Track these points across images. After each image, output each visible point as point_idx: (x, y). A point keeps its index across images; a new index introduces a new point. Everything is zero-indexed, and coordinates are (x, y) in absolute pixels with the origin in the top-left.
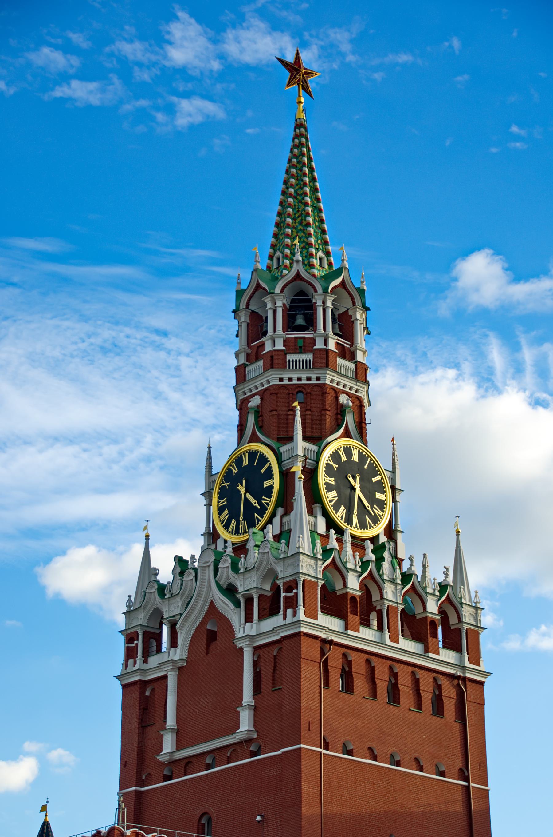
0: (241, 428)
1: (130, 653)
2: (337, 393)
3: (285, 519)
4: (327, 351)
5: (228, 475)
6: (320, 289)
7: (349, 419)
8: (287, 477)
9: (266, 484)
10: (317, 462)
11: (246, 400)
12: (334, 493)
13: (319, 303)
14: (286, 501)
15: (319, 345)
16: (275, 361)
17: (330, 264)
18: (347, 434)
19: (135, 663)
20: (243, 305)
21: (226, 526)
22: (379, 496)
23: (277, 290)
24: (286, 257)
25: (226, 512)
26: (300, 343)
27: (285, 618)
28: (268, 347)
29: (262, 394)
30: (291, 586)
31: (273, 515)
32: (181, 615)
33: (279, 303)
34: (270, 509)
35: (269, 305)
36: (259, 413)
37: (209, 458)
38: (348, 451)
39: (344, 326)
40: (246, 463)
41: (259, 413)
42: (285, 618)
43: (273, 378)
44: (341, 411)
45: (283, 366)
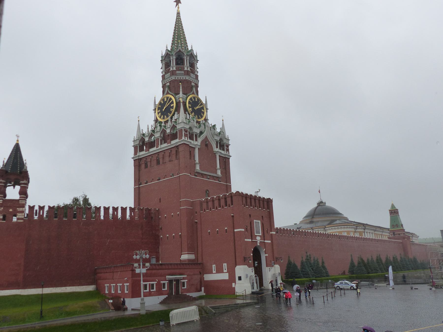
0: (163, 92)
2: (191, 82)
4: (188, 71)
5: (160, 103)
6: (185, 54)
7: (194, 89)
8: (178, 104)
9: (172, 105)
10: (186, 99)
11: (165, 84)
12: (191, 109)
13: (185, 58)
14: (177, 109)
15: (186, 69)
16: (173, 73)
17: (188, 49)
18: (193, 93)
20: (163, 59)
21: (160, 117)
22: (202, 110)
23: (174, 54)
26: (180, 68)
29: (170, 82)
30: (181, 131)
31: (174, 114)
33: (174, 58)
34: (172, 113)
35: (171, 58)
36: (169, 87)
37: (155, 100)
38: (194, 98)
39: (193, 65)
40: (166, 100)
41: (169, 87)
43: (173, 78)
44: (192, 87)
45: (176, 75)
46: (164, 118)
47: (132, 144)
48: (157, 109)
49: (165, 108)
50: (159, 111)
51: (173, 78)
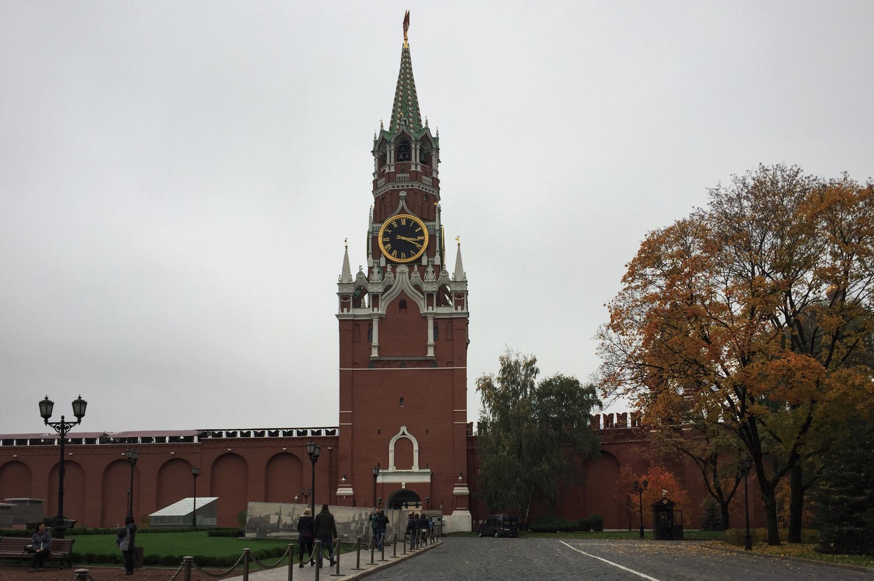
1: (343, 305)
3: (431, 259)
8: (432, 237)
15: (434, 175)
19: (348, 311)
21: (390, 252)
24: (410, 122)
25: (389, 245)
27: (456, 309)
28: (413, 168)
29: (408, 191)
31: (422, 255)
32: (383, 293)
33: (418, 147)
35: (413, 146)
36: (406, 199)
40: (404, 223)
42: (456, 309)
43: (416, 185)
45: (421, 181)
46: (399, 256)
47: (336, 289)
48: (381, 234)
49: (403, 238)
50: (388, 239)
51: (416, 185)
